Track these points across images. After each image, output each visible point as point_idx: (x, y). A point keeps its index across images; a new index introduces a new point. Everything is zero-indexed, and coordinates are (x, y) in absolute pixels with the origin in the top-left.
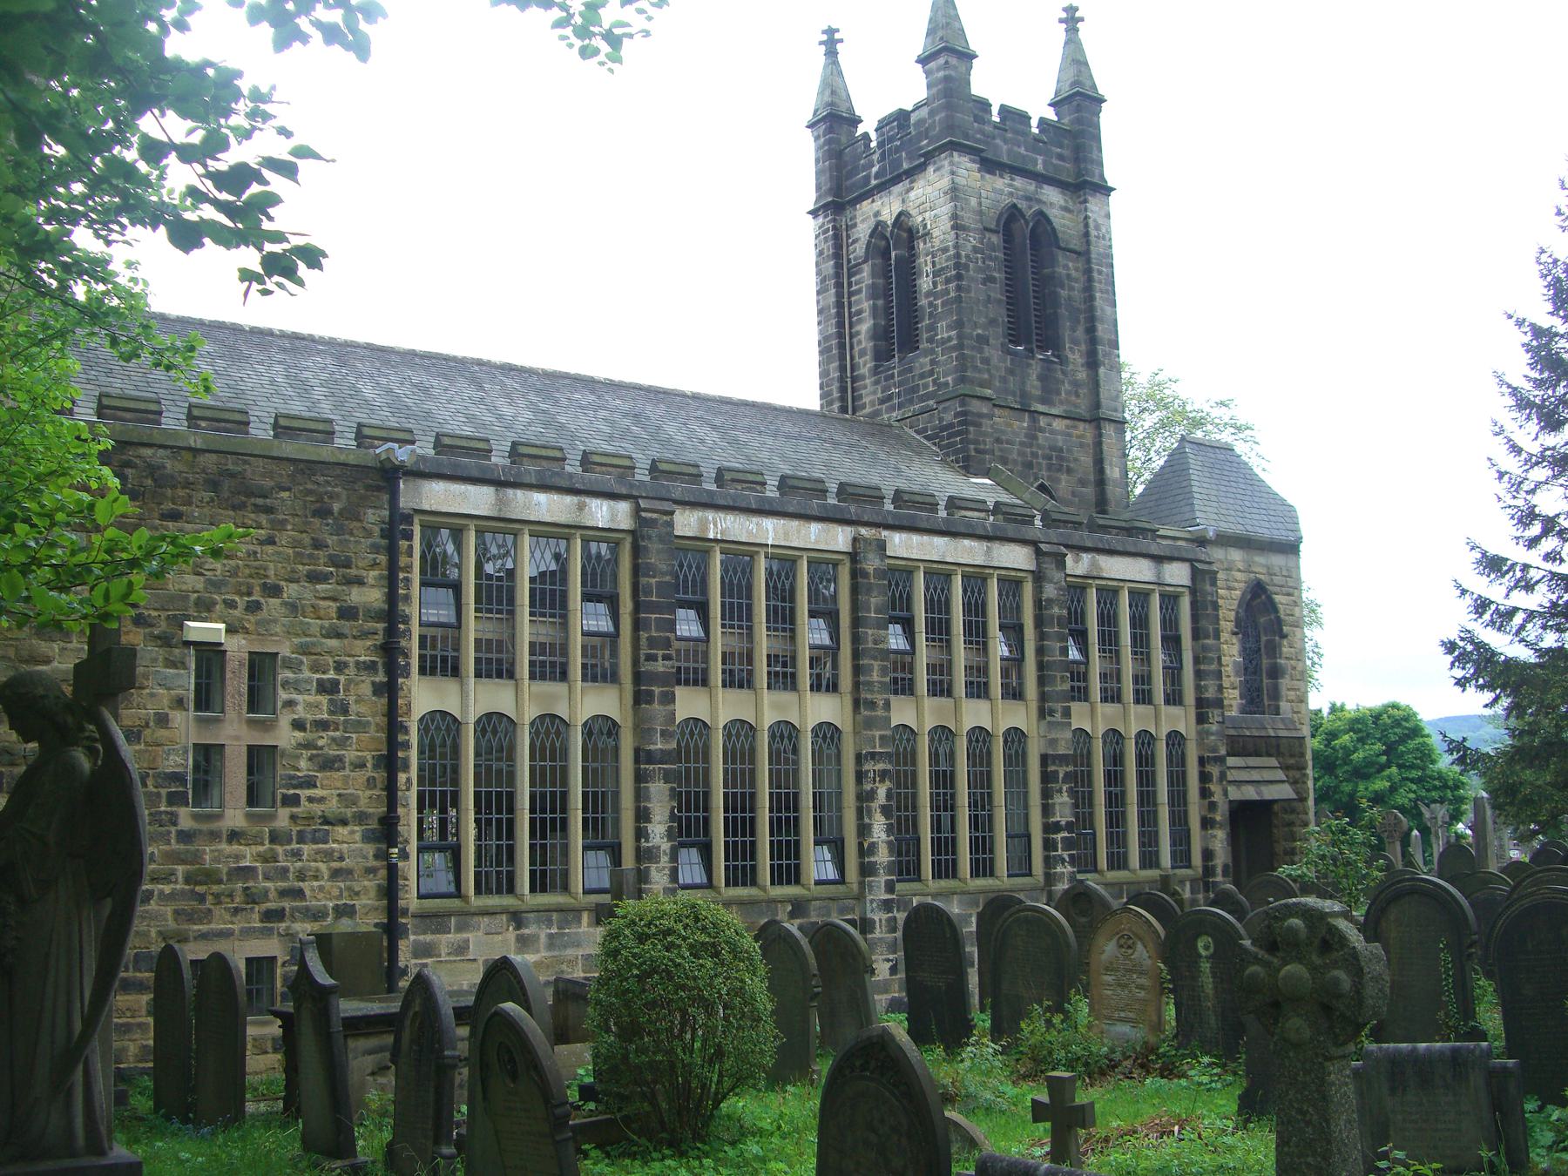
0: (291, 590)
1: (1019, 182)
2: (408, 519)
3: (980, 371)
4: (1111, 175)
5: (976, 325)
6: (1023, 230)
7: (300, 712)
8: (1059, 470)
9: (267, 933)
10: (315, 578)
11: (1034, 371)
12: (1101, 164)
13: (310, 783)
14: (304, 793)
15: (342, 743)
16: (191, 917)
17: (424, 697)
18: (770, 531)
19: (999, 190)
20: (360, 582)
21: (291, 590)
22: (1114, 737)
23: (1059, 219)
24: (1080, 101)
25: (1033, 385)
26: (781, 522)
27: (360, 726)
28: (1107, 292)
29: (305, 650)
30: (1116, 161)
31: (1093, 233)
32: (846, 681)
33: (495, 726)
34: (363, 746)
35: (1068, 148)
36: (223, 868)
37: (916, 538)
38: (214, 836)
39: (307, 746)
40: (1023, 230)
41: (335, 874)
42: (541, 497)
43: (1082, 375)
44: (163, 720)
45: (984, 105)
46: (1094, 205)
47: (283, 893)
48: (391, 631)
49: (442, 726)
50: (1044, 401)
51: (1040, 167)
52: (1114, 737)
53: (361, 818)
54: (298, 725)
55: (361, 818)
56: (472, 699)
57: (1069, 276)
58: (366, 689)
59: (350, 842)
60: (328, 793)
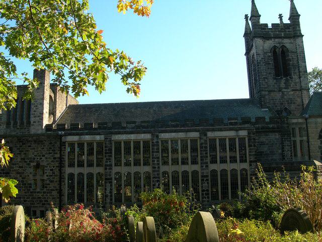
0: (46, 156)
1: (277, 40)
2: (64, 143)
3: (264, 85)
4: (303, 32)
5: (263, 75)
6: (278, 51)
7: (48, 174)
8: (291, 103)
9: (43, 207)
10: (50, 153)
11: (283, 81)
12: (300, 30)
13: (49, 184)
14: (48, 186)
15: (54, 178)
16: (32, 204)
17: (68, 170)
18: (132, 137)
19: (269, 44)
20: (57, 153)
21: (46, 156)
22: (129, 174)
23: (288, 46)
24: (295, 16)
25: (283, 85)
26: (135, 135)
27: (56, 176)
28: (303, 60)
29: (48, 164)
30: (304, 28)
31: (298, 47)
32: (151, 163)
33: (224, 172)
34: (57, 179)
35: (290, 30)
36: (37, 197)
37: (167, 134)
38: (35, 192)
39: (49, 179)
40: (278, 51)
41: (53, 198)
42: (87, 136)
43: (298, 80)
44: (28, 176)
45: (266, 25)
46: (298, 40)
47: (45, 201)
48: (61, 161)
49: (71, 176)
50: (285, 88)
51: (283, 35)
52: (129, 174)
53: (56, 190)
54: (47, 176)
55: (56, 190)
56: (76, 170)
57: (292, 58)
58: (57, 170)
59: (55, 193)
60: (52, 186)
